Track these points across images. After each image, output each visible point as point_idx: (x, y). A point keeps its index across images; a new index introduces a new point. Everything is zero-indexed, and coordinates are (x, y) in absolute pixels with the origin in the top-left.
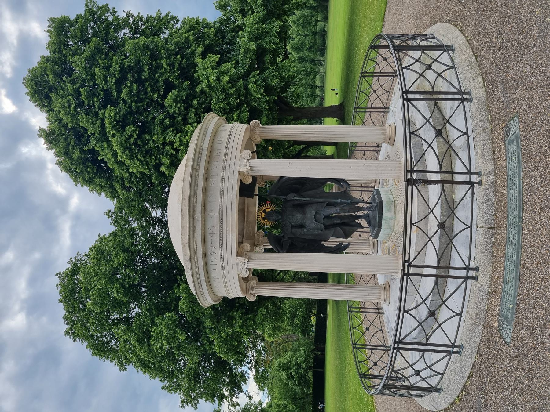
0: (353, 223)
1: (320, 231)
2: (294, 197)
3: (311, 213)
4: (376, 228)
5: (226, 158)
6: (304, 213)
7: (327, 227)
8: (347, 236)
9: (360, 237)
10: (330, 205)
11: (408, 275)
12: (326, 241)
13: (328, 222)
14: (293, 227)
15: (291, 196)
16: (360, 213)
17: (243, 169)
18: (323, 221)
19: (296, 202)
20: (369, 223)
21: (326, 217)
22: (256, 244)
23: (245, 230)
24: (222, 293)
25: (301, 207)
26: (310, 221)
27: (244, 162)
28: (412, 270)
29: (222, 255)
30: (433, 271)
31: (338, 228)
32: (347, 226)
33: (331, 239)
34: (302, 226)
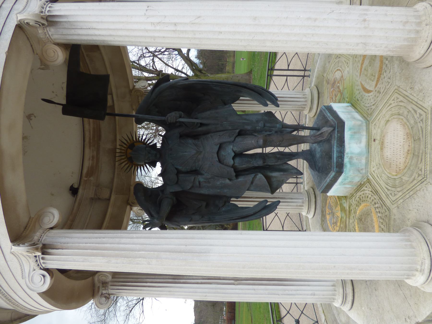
0: (285, 167)
1: (228, 181)
2: (180, 117)
3: (210, 145)
4: (332, 174)
7: (238, 173)
8: (273, 188)
9: (295, 192)
12: (237, 198)
14: (179, 172)
16: (293, 149)
18: (231, 162)
20: (313, 165)
22: (130, 202)
23: (115, 180)
31: (260, 176)
32: (272, 172)
33: (247, 194)
34: (196, 172)
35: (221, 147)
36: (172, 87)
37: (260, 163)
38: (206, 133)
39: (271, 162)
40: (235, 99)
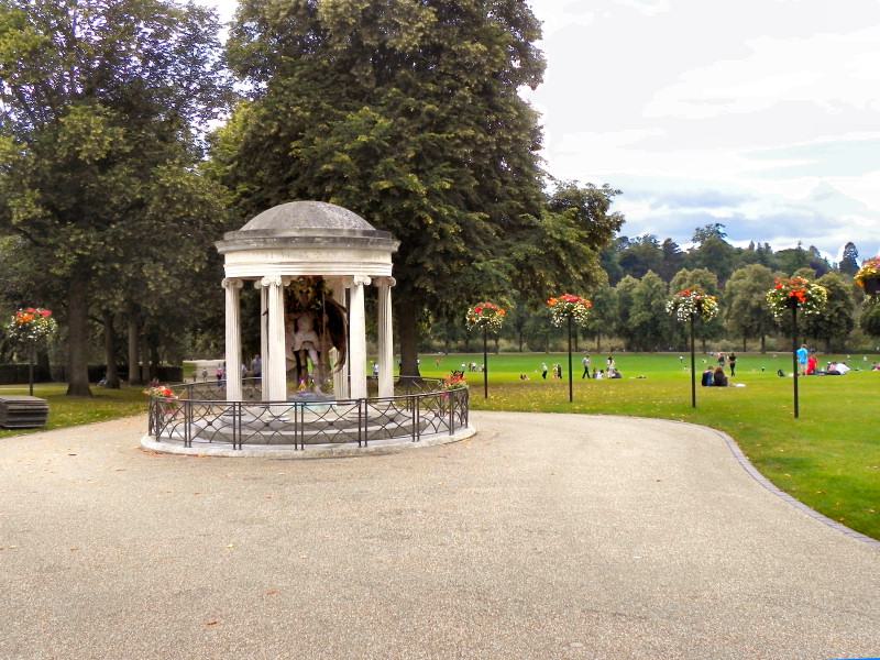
3: (312, 337)
5: (364, 263)
6: (309, 331)
10: (319, 354)
11: (295, 406)
13: (301, 355)
15: (325, 318)
17: (356, 280)
19: (319, 323)
21: (307, 353)
24: (229, 259)
25: (317, 329)
26: (305, 336)
27: (361, 279)
28: (299, 408)
29: (281, 263)
30: (299, 420)
35: (311, 343)
36: (341, 318)
37: (303, 363)
38: (318, 334)
39: (303, 372)
40: (338, 348)
